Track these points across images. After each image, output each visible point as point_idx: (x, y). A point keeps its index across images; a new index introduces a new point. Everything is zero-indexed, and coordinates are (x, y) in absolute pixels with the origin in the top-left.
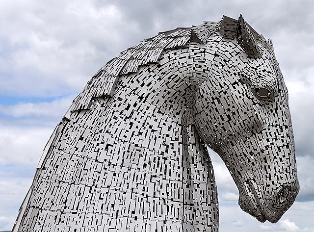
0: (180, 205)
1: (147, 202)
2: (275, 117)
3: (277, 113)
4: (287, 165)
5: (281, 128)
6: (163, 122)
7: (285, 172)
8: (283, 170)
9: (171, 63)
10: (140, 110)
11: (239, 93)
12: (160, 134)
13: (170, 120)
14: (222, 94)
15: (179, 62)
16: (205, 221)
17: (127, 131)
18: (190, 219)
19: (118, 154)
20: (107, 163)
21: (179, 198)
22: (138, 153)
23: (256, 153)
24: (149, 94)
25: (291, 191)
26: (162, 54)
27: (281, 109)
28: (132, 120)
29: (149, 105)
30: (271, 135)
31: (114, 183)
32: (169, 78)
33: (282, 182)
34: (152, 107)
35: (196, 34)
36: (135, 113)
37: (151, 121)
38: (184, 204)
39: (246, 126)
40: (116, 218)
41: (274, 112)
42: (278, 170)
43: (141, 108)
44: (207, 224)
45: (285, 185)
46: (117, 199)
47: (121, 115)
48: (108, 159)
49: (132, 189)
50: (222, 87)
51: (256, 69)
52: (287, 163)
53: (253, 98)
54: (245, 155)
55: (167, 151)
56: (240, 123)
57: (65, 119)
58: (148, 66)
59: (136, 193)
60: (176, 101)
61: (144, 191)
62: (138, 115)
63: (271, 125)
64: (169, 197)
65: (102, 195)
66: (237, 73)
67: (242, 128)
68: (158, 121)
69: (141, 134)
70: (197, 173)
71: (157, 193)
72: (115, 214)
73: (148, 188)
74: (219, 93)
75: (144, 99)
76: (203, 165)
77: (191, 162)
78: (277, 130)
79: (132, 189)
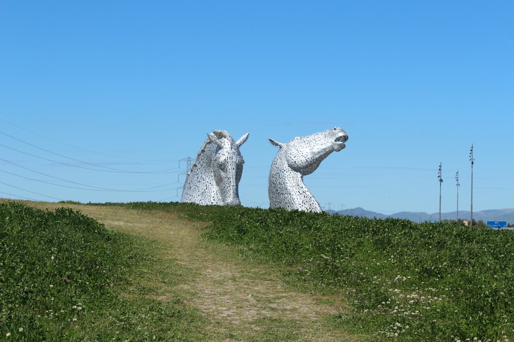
5: (229, 179)
6: (207, 176)
13: (209, 175)
20: (189, 195)
22: (198, 190)
23: (223, 189)
26: (206, 145)
33: (227, 202)
37: (203, 176)
48: (190, 193)
55: (207, 189)
57: (188, 174)
69: (200, 181)
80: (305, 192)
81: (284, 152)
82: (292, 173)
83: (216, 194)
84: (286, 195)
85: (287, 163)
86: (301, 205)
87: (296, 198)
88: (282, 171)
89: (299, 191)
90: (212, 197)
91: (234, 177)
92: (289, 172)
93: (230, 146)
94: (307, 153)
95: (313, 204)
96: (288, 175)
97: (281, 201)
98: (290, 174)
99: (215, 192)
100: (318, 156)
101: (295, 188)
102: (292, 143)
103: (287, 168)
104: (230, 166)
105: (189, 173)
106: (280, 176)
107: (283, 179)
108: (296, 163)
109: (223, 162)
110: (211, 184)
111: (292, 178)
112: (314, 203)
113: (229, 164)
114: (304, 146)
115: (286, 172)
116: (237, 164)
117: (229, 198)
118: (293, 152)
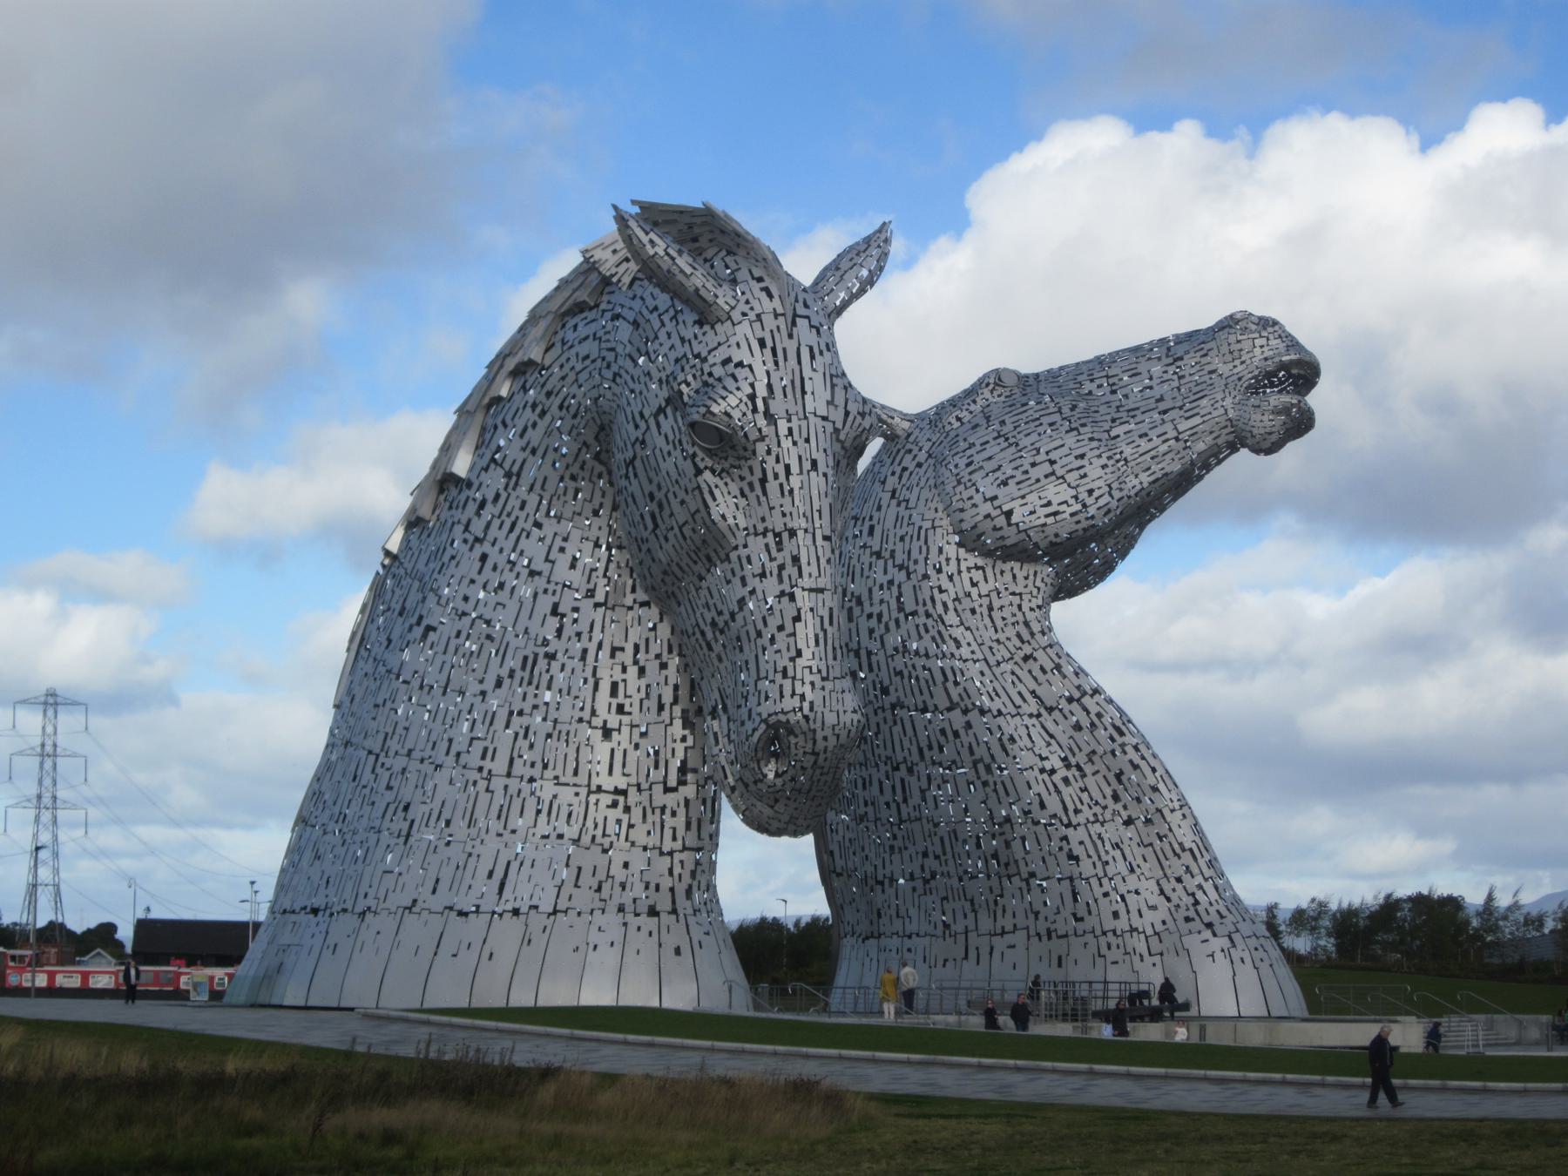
0: (577, 794)
1: (487, 790)
2: (760, 504)
3: (765, 493)
4: (786, 655)
5: (777, 535)
6: (559, 542)
7: (779, 676)
8: (775, 671)
9: (563, 359)
10: (505, 513)
11: (668, 443)
12: (549, 582)
14: (638, 446)
15: (577, 355)
16: (653, 840)
17: (472, 581)
18: (604, 835)
19: (445, 653)
20: (416, 684)
21: (576, 773)
23: (720, 621)
24: (524, 461)
25: (796, 736)
27: (776, 476)
28: (486, 547)
29: (524, 496)
30: (749, 562)
31: (420, 746)
32: (561, 407)
33: (767, 708)
34: (533, 500)
35: (595, 262)
36: (496, 523)
38: (589, 793)
39: (689, 541)
40: (406, 843)
41: (757, 486)
42: (763, 674)
43: (508, 508)
44: (660, 849)
45: (773, 719)
46: (420, 784)
47: (467, 535)
49: (458, 754)
50: (637, 427)
51: (705, 360)
52: (788, 649)
53: (694, 455)
54: (703, 633)
55: (559, 631)
56: (675, 535)
57: (388, 553)
58: (524, 373)
59: (464, 767)
60: (587, 474)
61: (483, 757)
62: (500, 528)
63: (752, 530)
64: (549, 774)
65: (394, 776)
66: (664, 379)
67: (682, 548)
68: (548, 541)
70: (643, 694)
71: (518, 763)
72: (404, 833)
73: (495, 749)
74: (633, 445)
75: (514, 478)
76: (664, 666)
77: (629, 660)
78: (767, 545)
79: (458, 754)
80: (1077, 695)
81: (922, 456)
82: (982, 584)
83: (633, 671)
84: (957, 718)
85: (946, 522)
86: (1054, 777)
87: (1023, 732)
88: (920, 569)
89: (1033, 692)
90: (605, 687)
91: (823, 525)
92: (965, 576)
93: (776, 303)
94: (1079, 463)
95: (1136, 767)
96: (961, 595)
97: (916, 757)
98: (974, 592)
99: (627, 656)
100: (1145, 479)
101: (1009, 678)
102: (972, 407)
103: (951, 550)
104: (787, 443)
105: (394, 546)
106: (909, 607)
107: (930, 622)
108: (1014, 519)
109: (736, 414)
110: (591, 602)
111: (986, 612)
112: (1142, 764)
113: (783, 430)
114: (1057, 417)
115: (943, 577)
116: (836, 431)
117: (787, 684)
118: (985, 455)
